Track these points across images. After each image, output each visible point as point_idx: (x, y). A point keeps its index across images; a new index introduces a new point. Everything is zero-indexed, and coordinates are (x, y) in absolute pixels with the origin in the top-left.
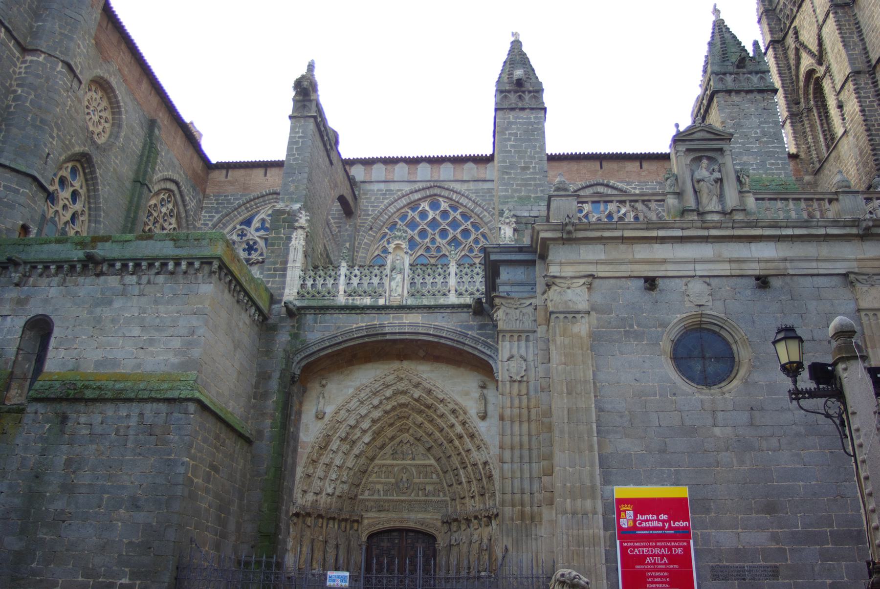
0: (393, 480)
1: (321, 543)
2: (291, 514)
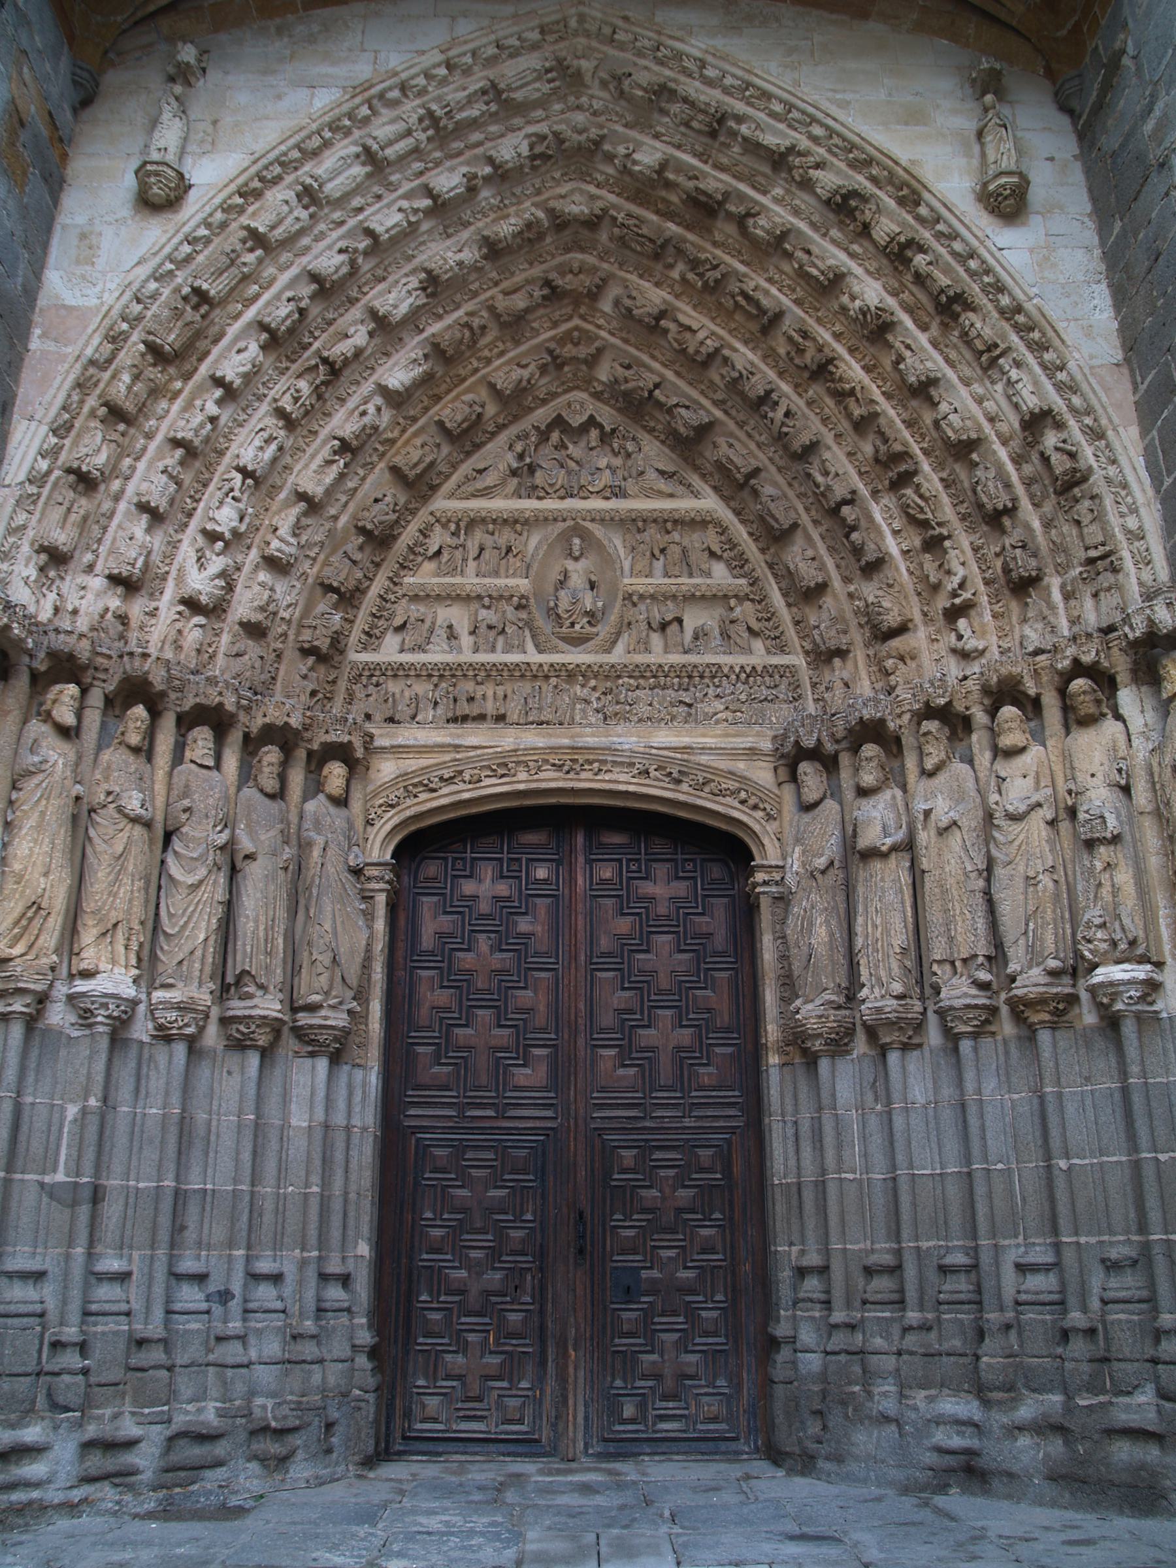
0: (522, 584)
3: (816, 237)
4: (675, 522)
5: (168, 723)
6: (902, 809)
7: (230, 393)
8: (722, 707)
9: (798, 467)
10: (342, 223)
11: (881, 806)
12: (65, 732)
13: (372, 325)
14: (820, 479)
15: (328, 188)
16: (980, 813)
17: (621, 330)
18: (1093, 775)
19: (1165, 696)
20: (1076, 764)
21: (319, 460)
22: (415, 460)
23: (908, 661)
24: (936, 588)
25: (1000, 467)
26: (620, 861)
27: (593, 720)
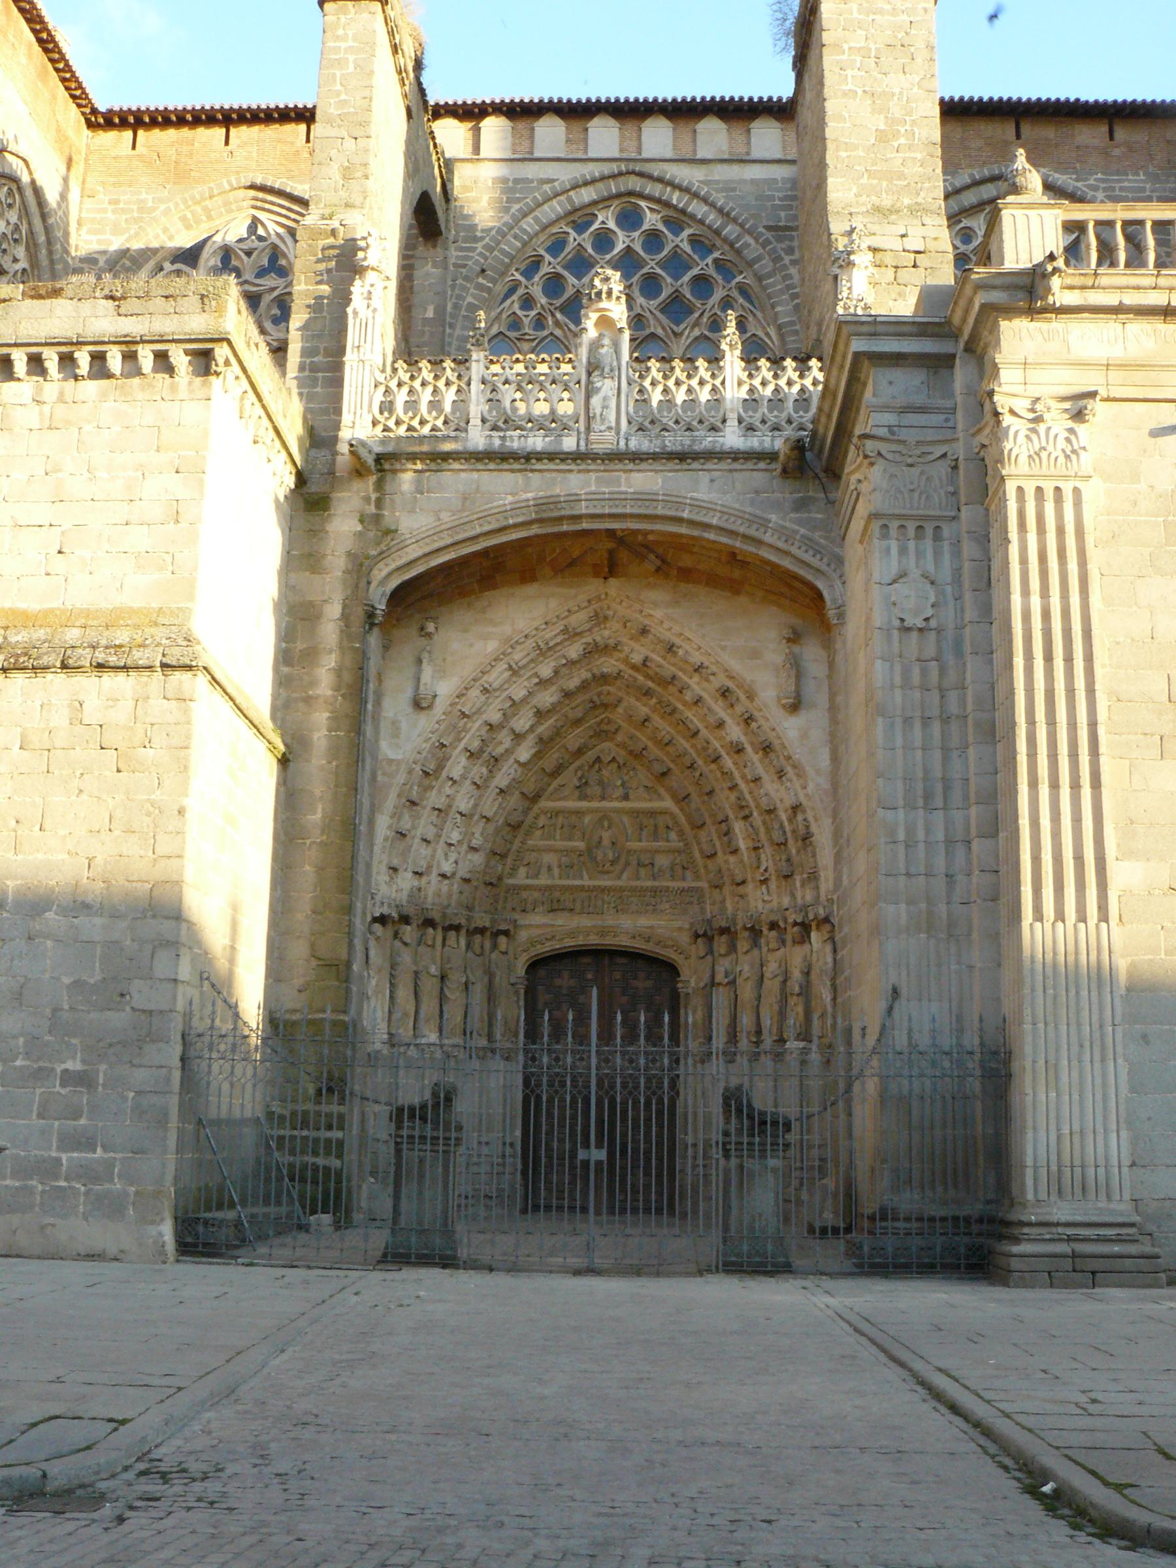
0: (581, 845)
2: (369, 919)
9: (706, 798)
12: (406, 944)
21: (491, 799)
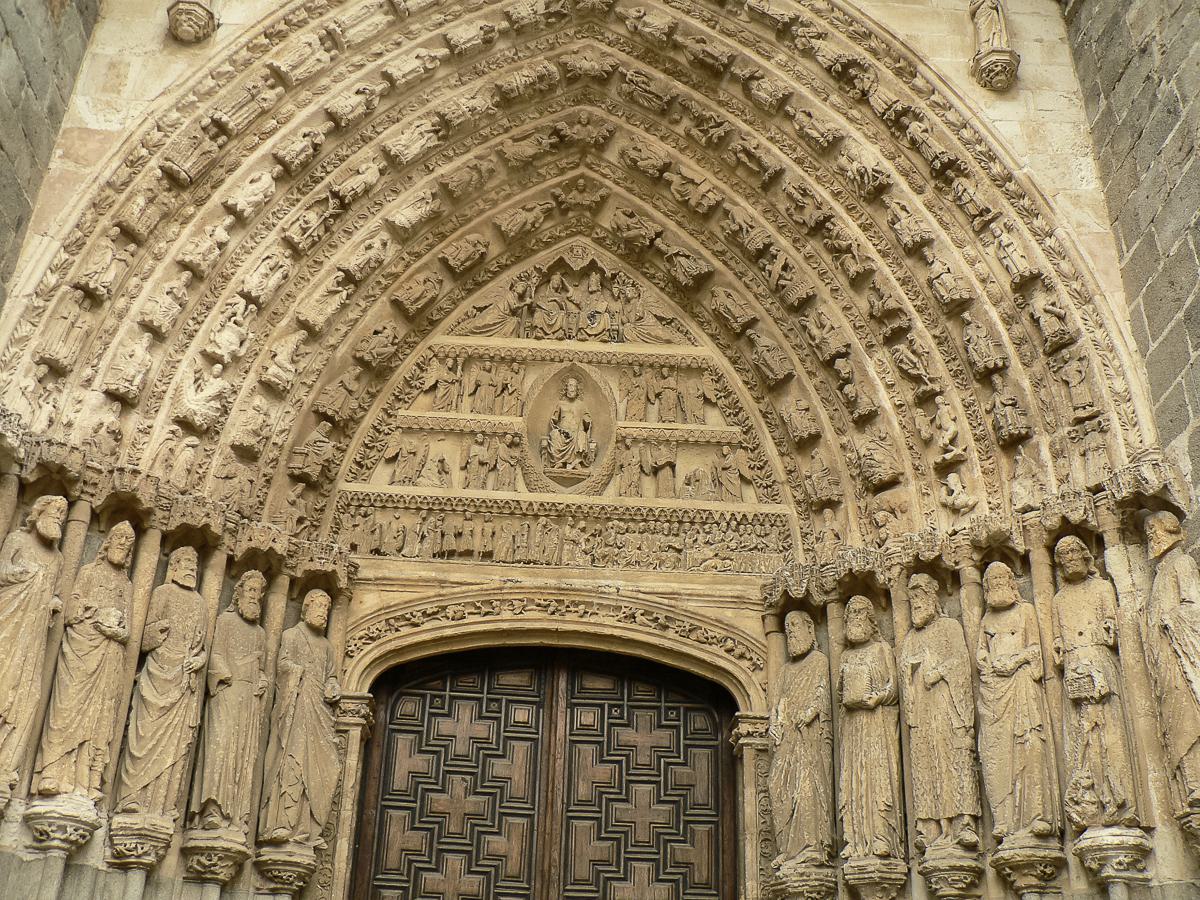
0: (516, 423)
1: (114, 646)
3: (817, 101)
4: (672, 368)
5: (153, 540)
6: (890, 663)
7: (239, 220)
8: (712, 554)
9: (793, 320)
10: (362, 66)
11: (868, 660)
12: (47, 543)
13: (384, 163)
14: (815, 331)
15: (350, 33)
16: (968, 670)
17: (625, 179)
18: (1081, 634)
19: (1152, 556)
20: (1063, 622)
21: (322, 290)
22: (417, 295)
23: (899, 514)
24: (928, 443)
25: (991, 326)
26: (602, 706)
27: (581, 562)
